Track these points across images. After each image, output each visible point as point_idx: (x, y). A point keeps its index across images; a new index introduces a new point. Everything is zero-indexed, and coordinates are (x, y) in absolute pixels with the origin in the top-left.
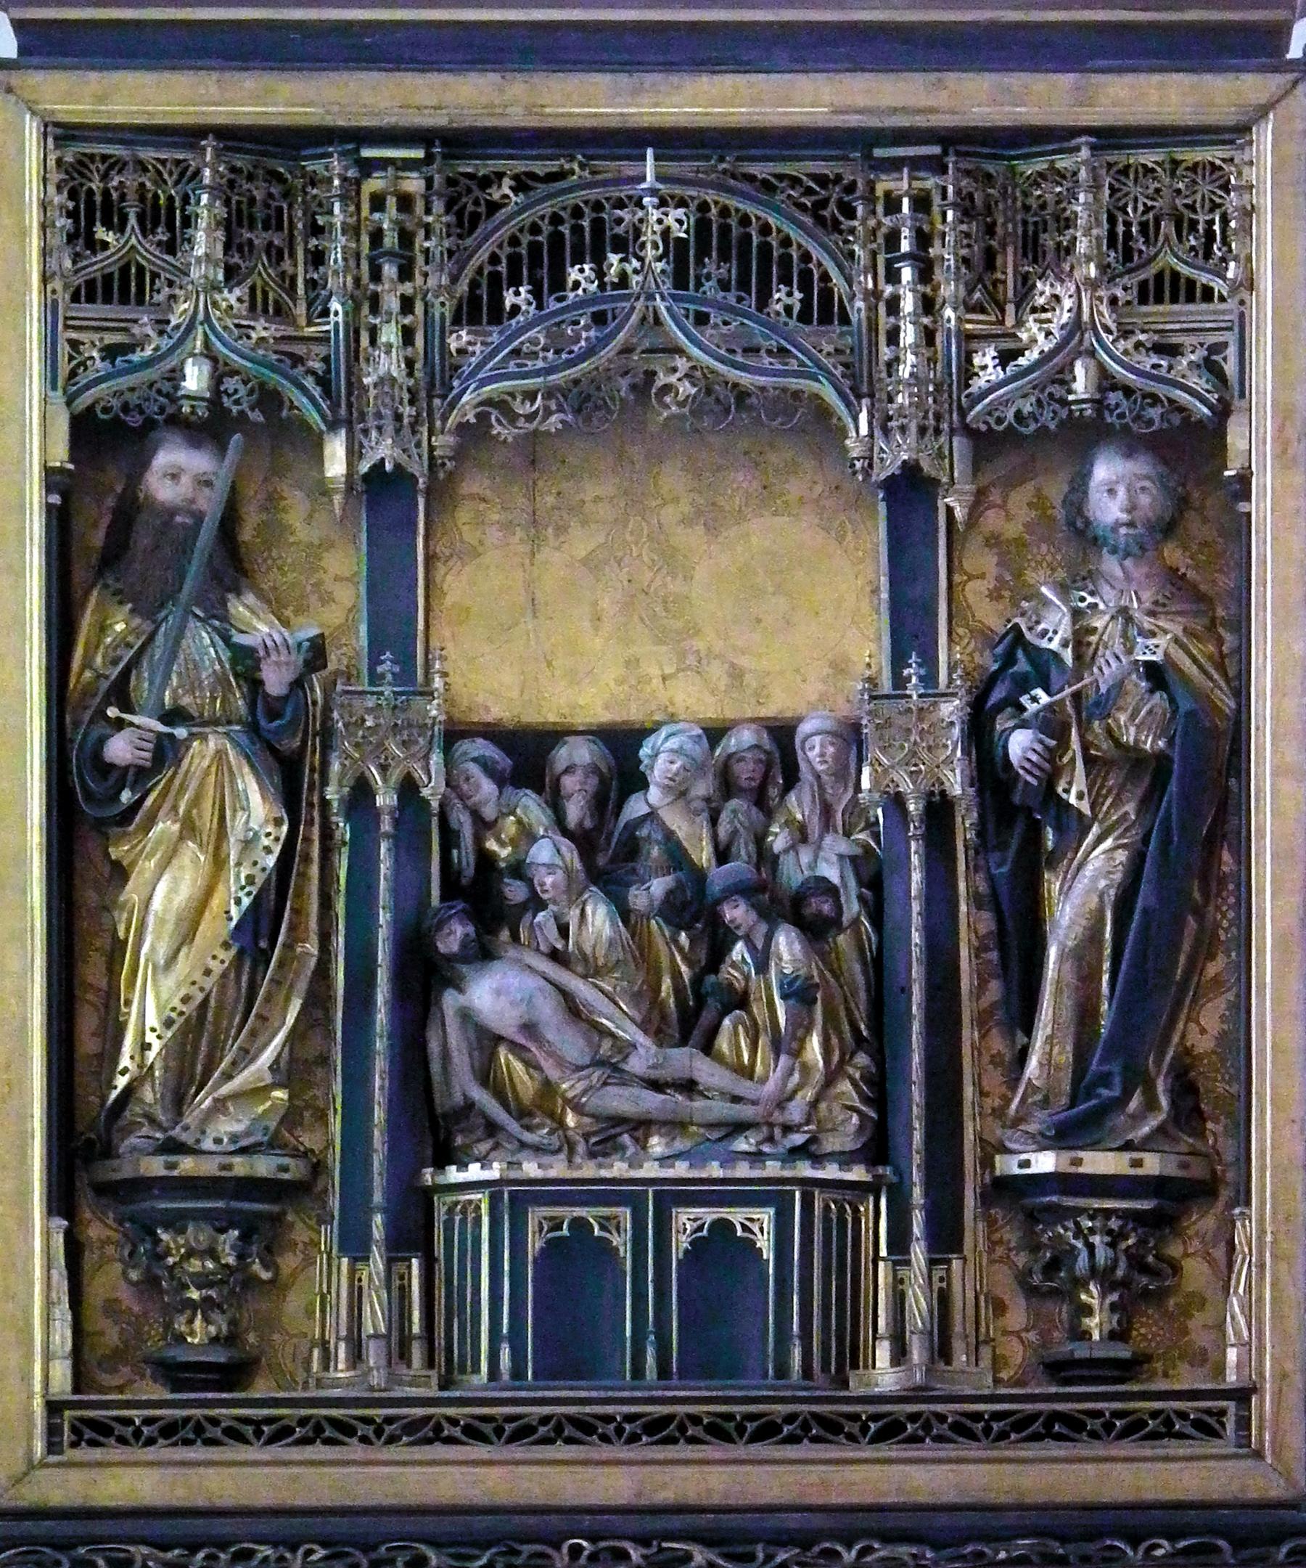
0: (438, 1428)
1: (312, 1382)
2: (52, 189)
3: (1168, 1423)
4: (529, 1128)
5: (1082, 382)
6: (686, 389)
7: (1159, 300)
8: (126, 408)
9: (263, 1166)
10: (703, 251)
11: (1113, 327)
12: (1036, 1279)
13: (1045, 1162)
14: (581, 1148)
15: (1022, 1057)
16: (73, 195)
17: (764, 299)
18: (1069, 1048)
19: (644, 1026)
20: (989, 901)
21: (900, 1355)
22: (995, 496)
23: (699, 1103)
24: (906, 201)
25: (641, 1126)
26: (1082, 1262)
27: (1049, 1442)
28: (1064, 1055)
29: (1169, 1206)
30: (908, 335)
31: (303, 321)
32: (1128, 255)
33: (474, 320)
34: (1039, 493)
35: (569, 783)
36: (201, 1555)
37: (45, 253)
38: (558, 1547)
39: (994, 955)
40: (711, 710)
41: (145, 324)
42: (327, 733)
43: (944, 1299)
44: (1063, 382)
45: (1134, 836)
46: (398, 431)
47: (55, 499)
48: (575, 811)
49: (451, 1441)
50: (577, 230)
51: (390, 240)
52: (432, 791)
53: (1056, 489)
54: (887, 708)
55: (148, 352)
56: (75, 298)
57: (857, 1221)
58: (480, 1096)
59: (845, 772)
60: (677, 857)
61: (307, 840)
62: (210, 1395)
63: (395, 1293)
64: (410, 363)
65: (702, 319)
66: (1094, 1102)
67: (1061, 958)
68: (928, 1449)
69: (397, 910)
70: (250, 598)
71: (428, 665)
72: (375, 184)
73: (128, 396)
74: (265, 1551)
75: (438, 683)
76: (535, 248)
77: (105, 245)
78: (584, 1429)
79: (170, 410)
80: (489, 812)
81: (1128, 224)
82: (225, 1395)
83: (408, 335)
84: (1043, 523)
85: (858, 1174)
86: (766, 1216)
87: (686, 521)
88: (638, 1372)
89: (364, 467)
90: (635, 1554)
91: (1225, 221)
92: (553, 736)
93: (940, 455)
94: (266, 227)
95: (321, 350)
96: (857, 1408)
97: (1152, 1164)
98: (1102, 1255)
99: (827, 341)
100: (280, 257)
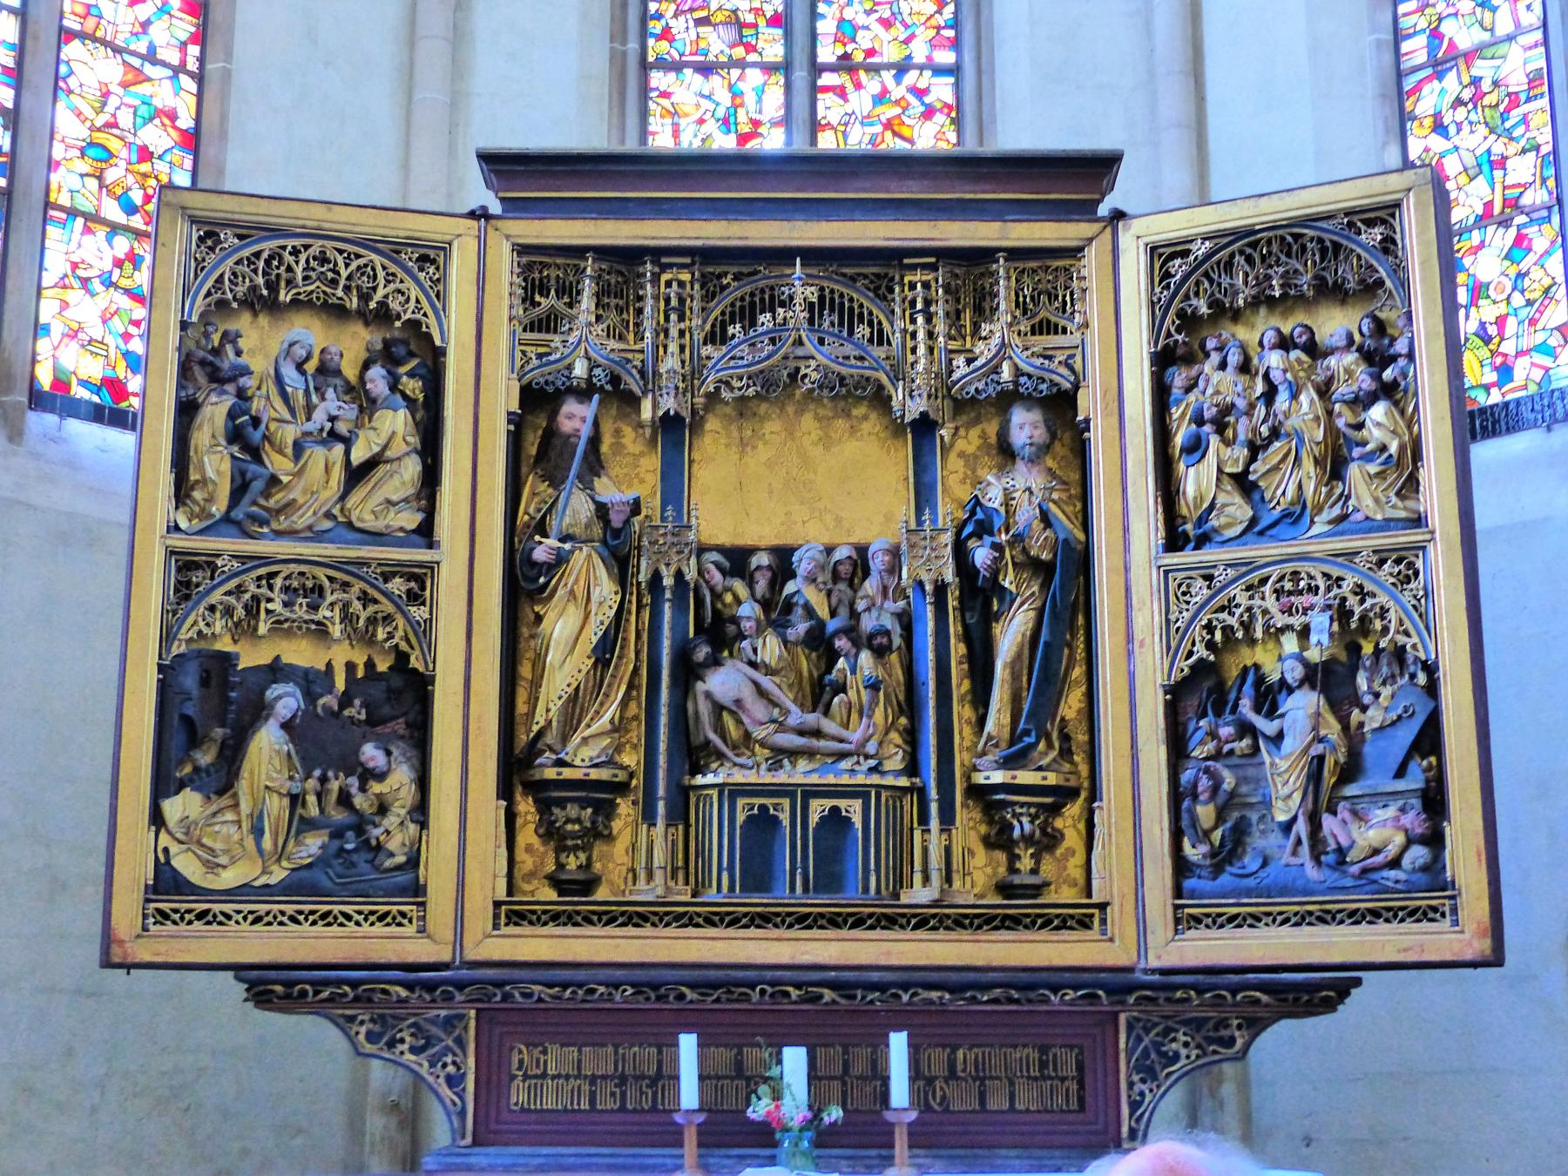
0: (691, 919)
1: (627, 892)
2: (515, 276)
3: (1064, 921)
4: (737, 755)
5: (1006, 373)
6: (815, 376)
7: (1041, 333)
8: (547, 383)
9: (603, 774)
10: (822, 309)
11: (1020, 345)
12: (993, 840)
13: (998, 777)
14: (764, 766)
15: (981, 722)
16: (525, 280)
17: (851, 332)
18: (1008, 715)
19: (795, 701)
20: (967, 637)
21: (926, 879)
22: (962, 432)
23: (823, 744)
24: (919, 285)
25: (794, 754)
26: (1017, 833)
27: (1002, 931)
28: (1007, 720)
29: (1061, 800)
30: (921, 350)
31: (632, 342)
32: (1025, 313)
33: (713, 342)
34: (983, 431)
35: (758, 575)
36: (569, 991)
37: (511, 307)
38: (754, 990)
39: (965, 666)
40: (827, 539)
41: (557, 338)
42: (639, 548)
43: (948, 850)
44: (997, 373)
45: (1038, 604)
46: (676, 395)
47: (512, 427)
48: (762, 586)
49: (697, 925)
50: (762, 300)
51: (674, 302)
52: (691, 575)
53: (992, 428)
54: (914, 539)
55: (558, 356)
56: (525, 330)
57: (902, 807)
58: (712, 736)
59: (894, 568)
60: (809, 611)
61: (630, 602)
62: (576, 899)
63: (670, 843)
64: (683, 362)
65: (821, 341)
66: (1022, 745)
67: (1004, 668)
68: (941, 934)
69: (673, 639)
70: (604, 479)
71: (689, 513)
72: (665, 277)
73: (547, 377)
74: (602, 989)
75: (693, 521)
76: (742, 308)
77: (539, 304)
78: (763, 920)
79: (568, 384)
80: (719, 588)
81: (1025, 297)
82: (583, 899)
83: (682, 348)
84: (985, 446)
85: (903, 782)
86: (857, 804)
87: (814, 444)
88: (793, 889)
89: (660, 413)
90: (794, 993)
91: (1072, 294)
92: (751, 551)
93: (938, 410)
94: (616, 297)
95: (640, 356)
96: (906, 911)
97: (1052, 779)
98: (1027, 827)
99: (879, 352)
100: (622, 313)
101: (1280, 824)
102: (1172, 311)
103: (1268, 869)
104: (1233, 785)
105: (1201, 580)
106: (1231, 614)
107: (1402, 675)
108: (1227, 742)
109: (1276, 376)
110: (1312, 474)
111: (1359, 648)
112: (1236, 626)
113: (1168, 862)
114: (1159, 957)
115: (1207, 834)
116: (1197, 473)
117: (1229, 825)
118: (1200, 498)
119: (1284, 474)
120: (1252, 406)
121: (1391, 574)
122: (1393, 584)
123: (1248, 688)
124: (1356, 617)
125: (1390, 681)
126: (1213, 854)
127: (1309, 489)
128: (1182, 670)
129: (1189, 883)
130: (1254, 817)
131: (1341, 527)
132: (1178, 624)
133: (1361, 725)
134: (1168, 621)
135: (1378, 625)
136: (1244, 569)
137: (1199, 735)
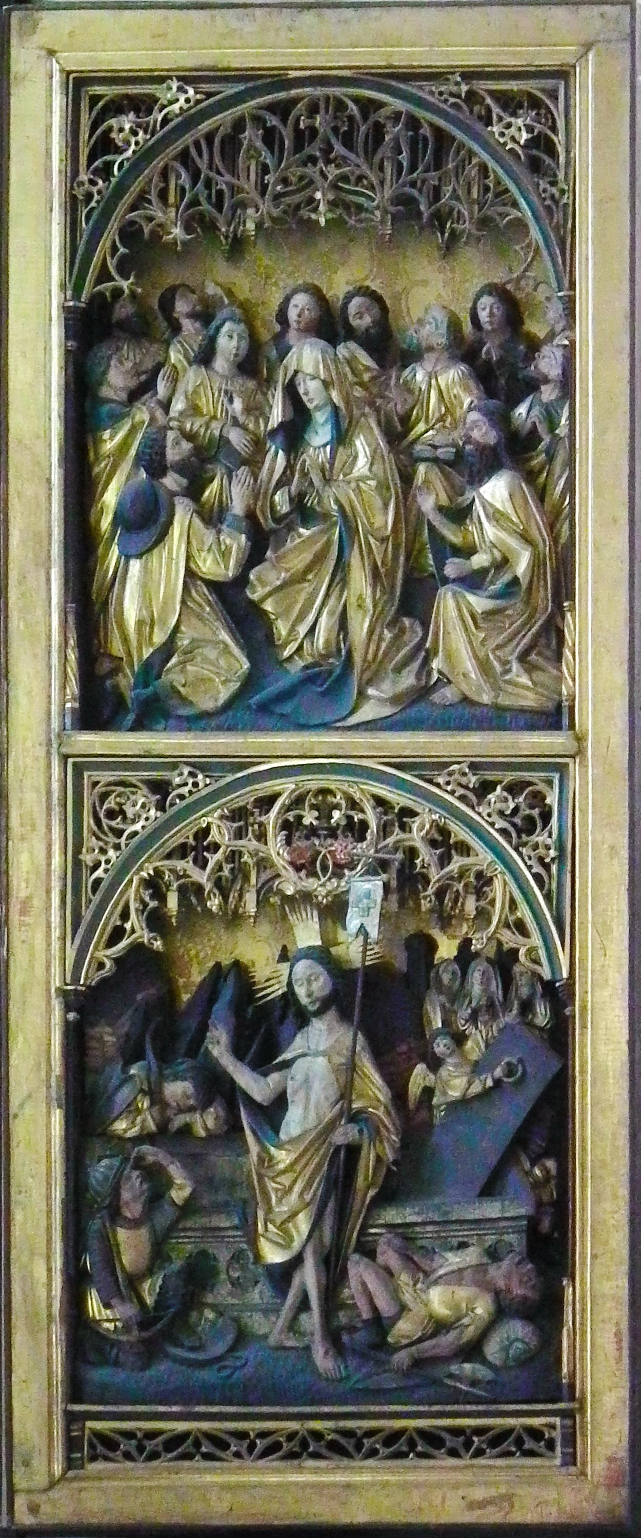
101: (271, 1270)
102: (111, 233)
103: (242, 1353)
104: (187, 1192)
105: (145, 790)
106: (202, 863)
107: (506, 1005)
108: (181, 1111)
109: (311, 391)
110: (369, 602)
111: (431, 946)
112: (208, 886)
113: (58, 1332)
114: (34, 1509)
115: (134, 1281)
116: (146, 571)
117: (177, 1265)
118: (146, 624)
119: (315, 592)
120: (259, 445)
121: (501, 813)
122: (503, 832)
123: (221, 1008)
124: (430, 890)
125: (483, 1017)
126: (146, 1320)
127: (360, 626)
128: (101, 966)
129: (99, 1375)
130: (223, 1256)
131: (413, 712)
132: (99, 873)
133: (428, 1092)
134: (77, 863)
135: (471, 905)
136: (230, 778)
137: (125, 1094)
